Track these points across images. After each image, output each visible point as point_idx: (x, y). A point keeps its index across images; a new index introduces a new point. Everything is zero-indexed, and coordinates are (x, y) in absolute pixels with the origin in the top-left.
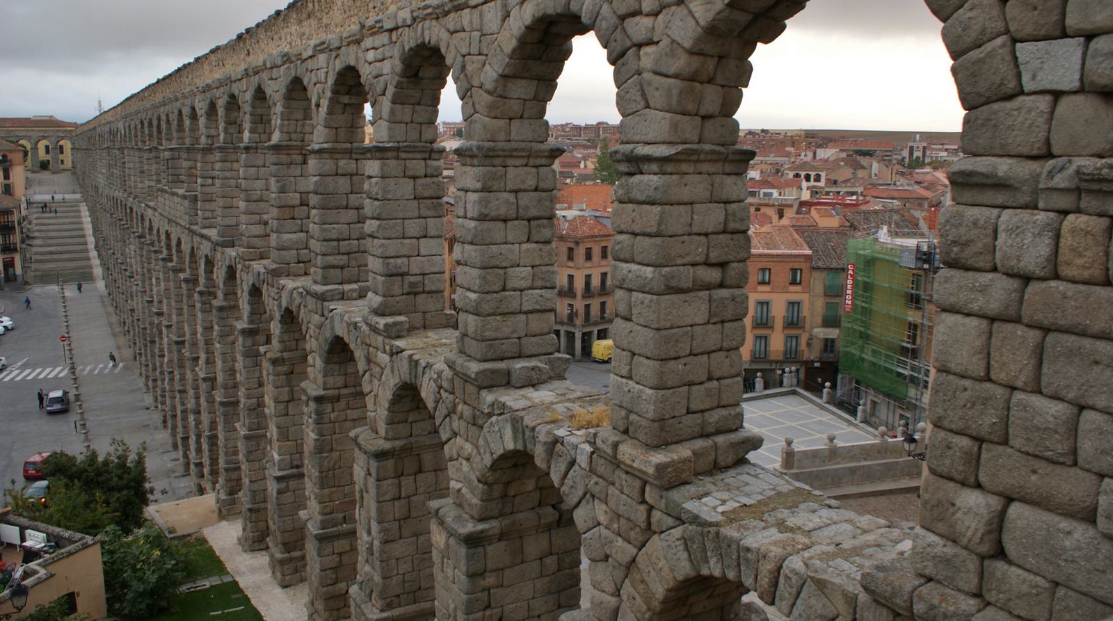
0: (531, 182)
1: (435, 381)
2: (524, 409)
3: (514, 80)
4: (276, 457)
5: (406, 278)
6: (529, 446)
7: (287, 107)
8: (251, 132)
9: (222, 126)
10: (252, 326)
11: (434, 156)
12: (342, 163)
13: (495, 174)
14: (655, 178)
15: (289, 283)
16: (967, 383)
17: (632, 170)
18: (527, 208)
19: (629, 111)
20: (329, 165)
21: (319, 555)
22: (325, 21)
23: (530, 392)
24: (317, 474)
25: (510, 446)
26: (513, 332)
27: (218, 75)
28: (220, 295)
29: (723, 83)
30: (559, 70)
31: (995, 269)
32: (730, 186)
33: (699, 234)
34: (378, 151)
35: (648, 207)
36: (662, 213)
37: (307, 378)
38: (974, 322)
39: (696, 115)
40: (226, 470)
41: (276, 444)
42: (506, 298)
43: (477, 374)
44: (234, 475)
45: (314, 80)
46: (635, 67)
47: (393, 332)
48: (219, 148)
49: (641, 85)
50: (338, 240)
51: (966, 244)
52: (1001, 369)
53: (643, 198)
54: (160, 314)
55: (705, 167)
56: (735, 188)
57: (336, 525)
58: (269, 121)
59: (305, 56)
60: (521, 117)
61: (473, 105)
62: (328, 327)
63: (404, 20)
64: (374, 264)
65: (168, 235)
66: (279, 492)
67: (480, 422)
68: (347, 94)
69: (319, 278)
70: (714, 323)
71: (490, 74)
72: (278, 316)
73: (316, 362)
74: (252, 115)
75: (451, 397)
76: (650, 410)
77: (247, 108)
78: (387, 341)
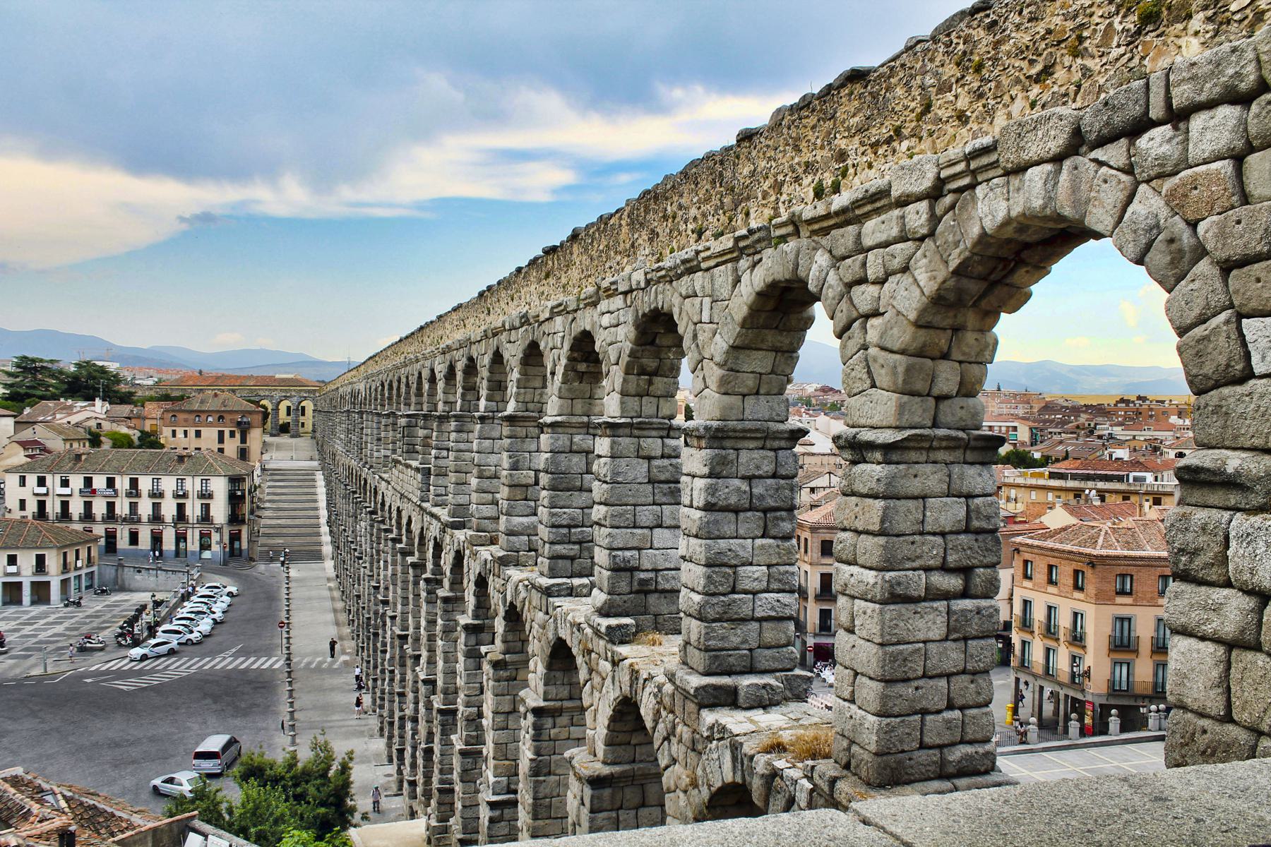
0: (767, 468)
1: (655, 696)
2: (745, 734)
3: (748, 352)
4: (492, 779)
5: (636, 573)
6: (747, 778)
8: (489, 399)
9: (460, 391)
10: (476, 622)
11: (672, 433)
12: (577, 439)
13: (725, 458)
14: (879, 468)
15: (515, 574)
16: (1205, 723)
17: (857, 458)
18: (761, 497)
19: (855, 391)
20: (563, 440)
22: (564, 280)
23: (758, 715)
24: (531, 801)
25: (729, 778)
26: (742, 643)
28: (446, 583)
29: (961, 358)
30: (801, 340)
31: (1228, 584)
32: (974, 478)
33: (934, 534)
34: (612, 429)
35: (870, 501)
36: (886, 509)
37: (528, 686)
38: (1209, 647)
39: (928, 395)
40: (439, 790)
41: (491, 763)
42: (734, 601)
43: (697, 689)
45: (550, 345)
46: (862, 341)
47: (618, 636)
48: (455, 416)
49: (866, 360)
50: (569, 527)
51: (1195, 553)
52: (1243, 709)
53: (865, 491)
54: (386, 603)
55: (941, 455)
56: (979, 479)
59: (542, 319)
60: (757, 393)
61: (704, 378)
62: (552, 626)
63: (639, 283)
64: (601, 556)
65: (399, 511)
66: (491, 820)
67: (700, 747)
68: (585, 361)
69: (546, 570)
70: (955, 640)
71: (719, 346)
72: (501, 612)
73: (537, 668)
75: (671, 716)
76: (871, 740)
77: (484, 373)
78: (609, 646)
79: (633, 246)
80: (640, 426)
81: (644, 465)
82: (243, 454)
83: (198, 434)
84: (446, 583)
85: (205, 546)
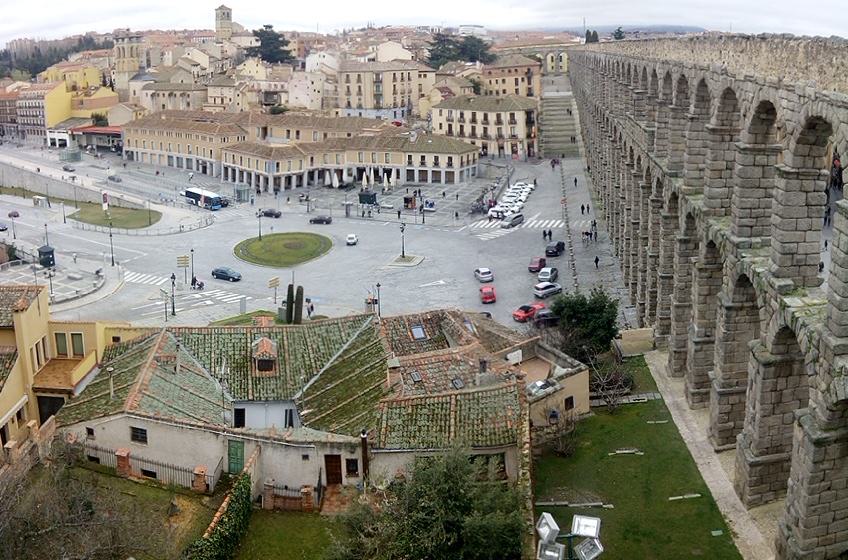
4: (696, 329)
7: (723, 103)
10: (687, 238)
12: (758, 158)
20: (750, 159)
21: (719, 404)
27: (673, 57)
28: (666, 206)
34: (785, 175)
44: (666, 322)
45: (743, 97)
57: (731, 387)
58: (709, 101)
65: (632, 150)
66: (696, 351)
74: (697, 96)
78: (779, 296)
79: (807, 68)
80: (803, 174)
81: (804, 194)
82: (530, 94)
83: (504, 81)
84: (666, 206)
85: (514, 152)
